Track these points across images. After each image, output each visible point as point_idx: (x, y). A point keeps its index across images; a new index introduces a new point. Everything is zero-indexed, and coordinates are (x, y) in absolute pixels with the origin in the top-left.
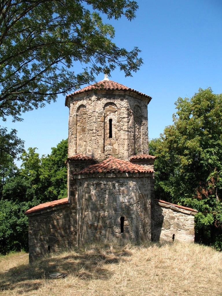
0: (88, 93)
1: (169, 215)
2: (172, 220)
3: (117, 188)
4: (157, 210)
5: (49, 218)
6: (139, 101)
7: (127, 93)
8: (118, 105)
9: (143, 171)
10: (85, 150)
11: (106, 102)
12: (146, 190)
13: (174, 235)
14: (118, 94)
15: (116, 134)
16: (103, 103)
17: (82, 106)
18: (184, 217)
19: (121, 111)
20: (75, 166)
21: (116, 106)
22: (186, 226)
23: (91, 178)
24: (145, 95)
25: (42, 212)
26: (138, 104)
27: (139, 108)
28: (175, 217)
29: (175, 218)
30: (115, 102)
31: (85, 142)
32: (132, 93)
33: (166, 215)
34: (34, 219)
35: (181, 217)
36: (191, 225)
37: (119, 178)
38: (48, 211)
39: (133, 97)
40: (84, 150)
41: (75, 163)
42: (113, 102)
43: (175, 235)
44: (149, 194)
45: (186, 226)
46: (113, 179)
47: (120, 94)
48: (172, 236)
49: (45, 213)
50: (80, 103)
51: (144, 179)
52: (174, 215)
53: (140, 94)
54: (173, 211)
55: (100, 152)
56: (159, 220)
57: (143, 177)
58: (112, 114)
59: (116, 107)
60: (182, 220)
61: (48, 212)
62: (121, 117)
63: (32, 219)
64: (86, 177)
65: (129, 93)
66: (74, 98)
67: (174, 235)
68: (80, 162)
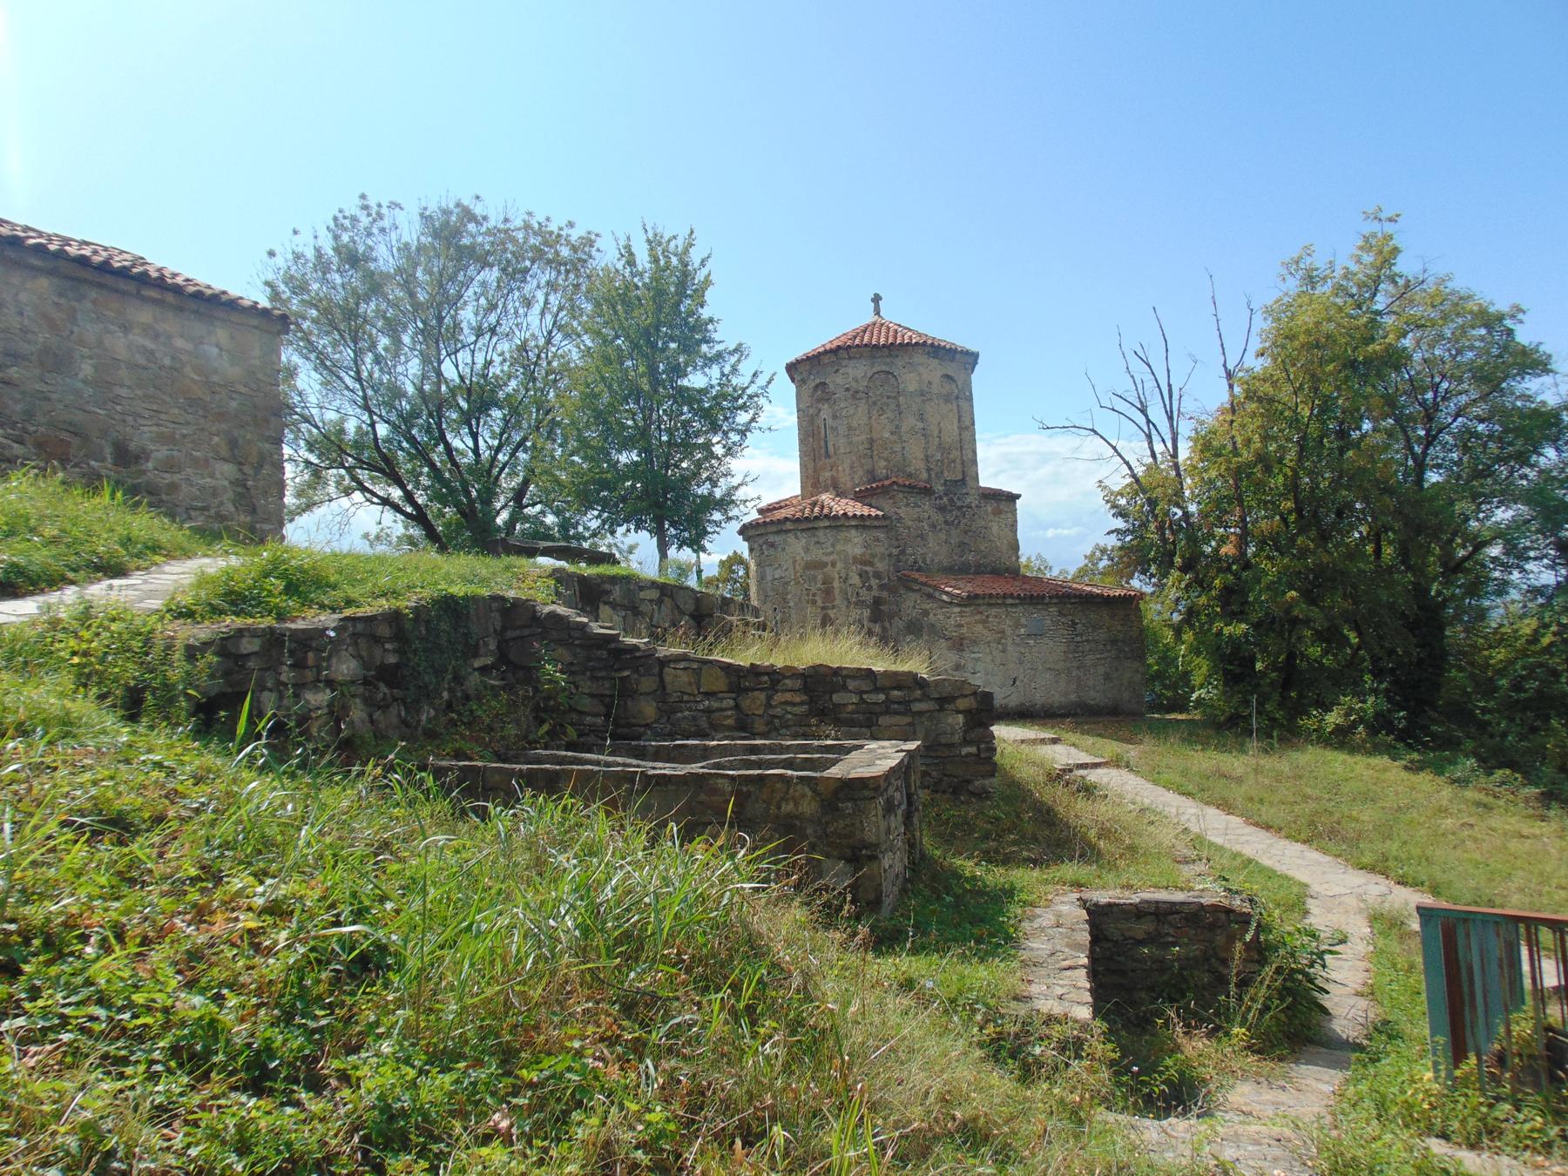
26: (884, 368)
51: (820, 533)
60: (941, 617)
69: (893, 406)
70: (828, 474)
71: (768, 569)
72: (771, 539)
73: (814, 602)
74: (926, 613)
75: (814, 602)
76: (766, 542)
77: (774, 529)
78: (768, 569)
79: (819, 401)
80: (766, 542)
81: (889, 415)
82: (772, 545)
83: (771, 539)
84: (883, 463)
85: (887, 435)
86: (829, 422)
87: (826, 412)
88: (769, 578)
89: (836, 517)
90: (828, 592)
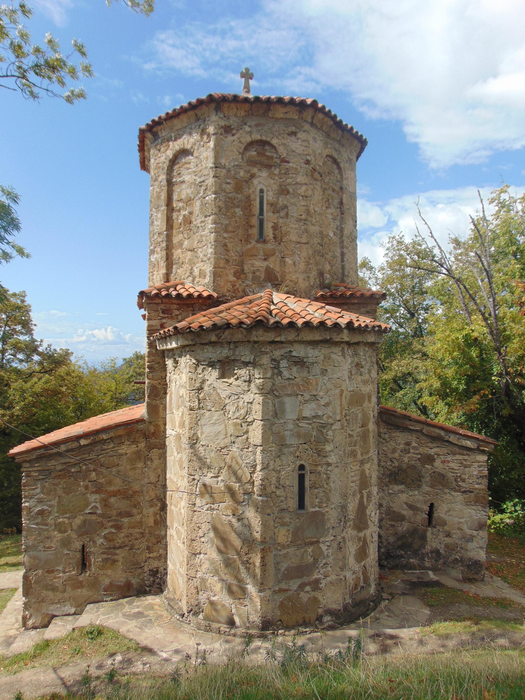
0: (198, 112)
1: (417, 452)
2: (426, 466)
3: (286, 374)
4: (387, 436)
5: (86, 465)
6: (337, 146)
7: (308, 114)
8: (281, 150)
9: (363, 325)
10: (191, 273)
11: (249, 139)
12: (365, 382)
13: (432, 506)
14: (282, 116)
15: (275, 227)
16: (240, 142)
17: (184, 152)
18: (458, 457)
19: (291, 164)
20: (161, 315)
21: (277, 152)
22: (463, 480)
23: (205, 344)
24: (352, 128)
25: (63, 448)
27: (335, 166)
28: (436, 456)
29: (434, 460)
30: (274, 142)
31: (190, 253)
32: (321, 116)
33: (412, 451)
34: (39, 468)
35: (449, 458)
36: (478, 478)
37: (291, 343)
38: (83, 442)
39: (320, 129)
40: (188, 274)
41: (162, 306)
42: (268, 139)
43: (435, 505)
44: (372, 393)
45: (463, 480)
46: (273, 346)
47: (288, 116)
48: (426, 508)
49: (72, 450)
50: (175, 146)
51: (361, 351)
52: (432, 452)
53: (339, 125)
54: (428, 440)
55: (232, 278)
56: (391, 466)
57: (358, 343)
58: (264, 174)
59: (275, 156)
61: (81, 447)
62: (289, 181)
63: (36, 469)
64: (190, 343)
65: (313, 118)
66: (159, 133)
67: (432, 506)
68: (175, 301)
69: (336, 202)
70: (259, 264)
71: (289, 402)
72: (299, 351)
73: (353, 454)
74: (430, 459)
75: (353, 454)
76: (288, 356)
77: (317, 336)
78: (289, 402)
79: (252, 163)
80: (288, 356)
81: (331, 210)
82: (300, 363)
83: (299, 351)
84: (327, 267)
85: (332, 235)
86: (269, 196)
87: (263, 182)
88: (291, 415)
89: (277, 325)
90: (364, 436)
